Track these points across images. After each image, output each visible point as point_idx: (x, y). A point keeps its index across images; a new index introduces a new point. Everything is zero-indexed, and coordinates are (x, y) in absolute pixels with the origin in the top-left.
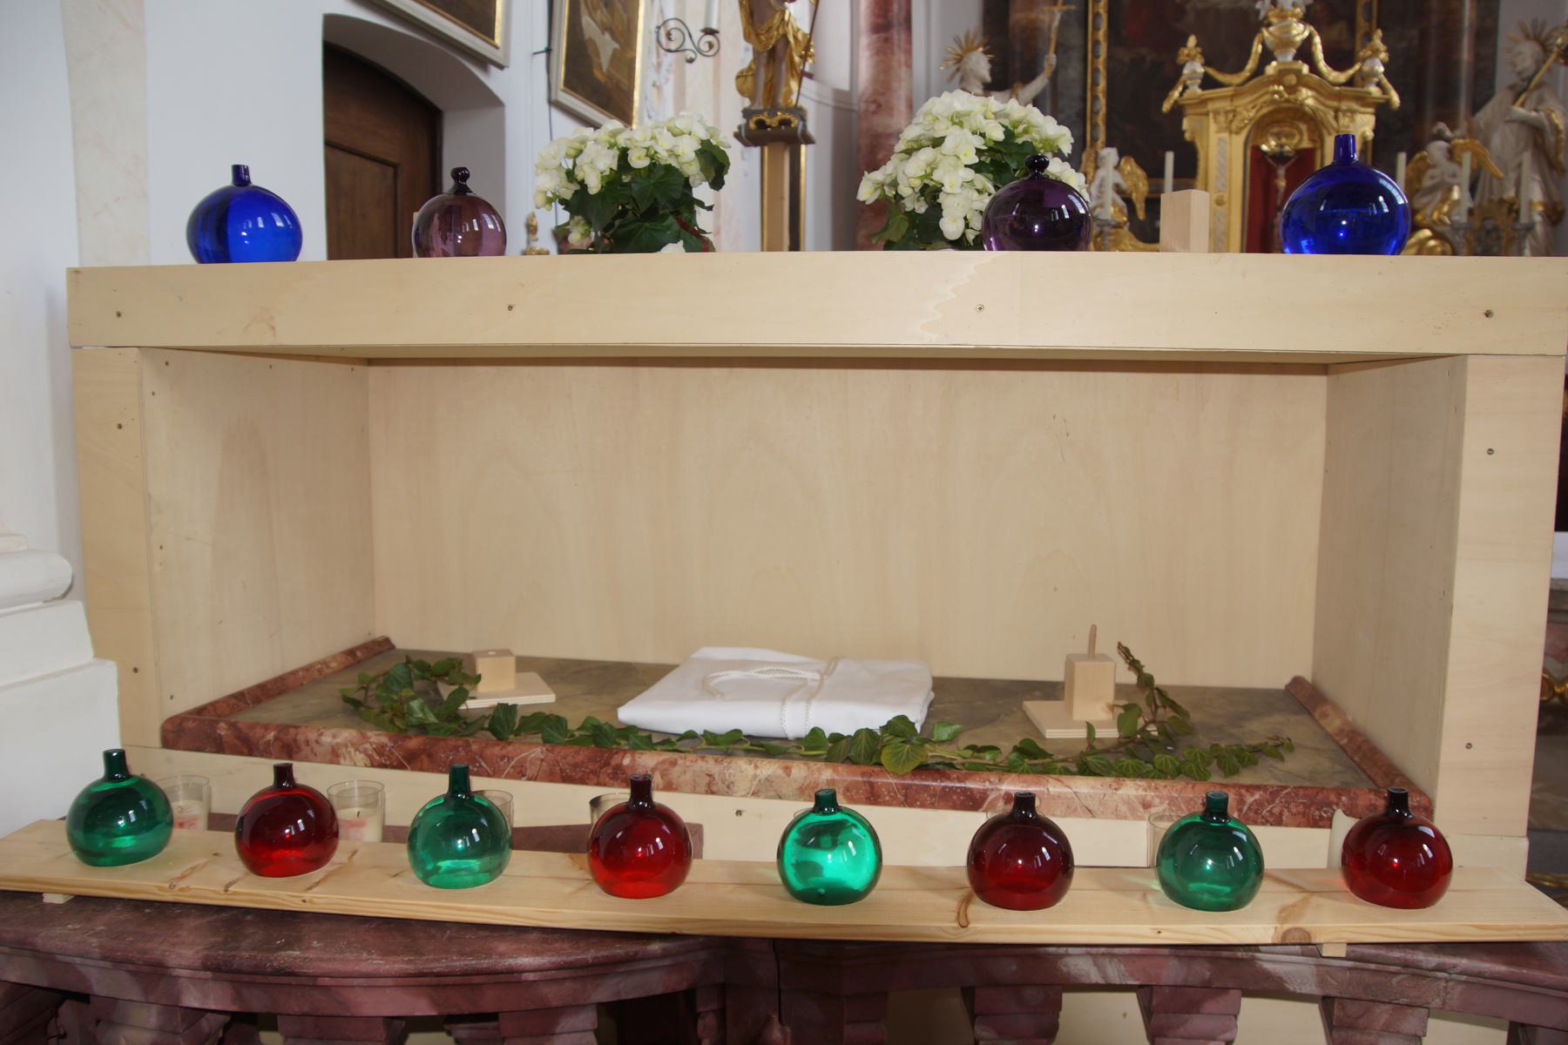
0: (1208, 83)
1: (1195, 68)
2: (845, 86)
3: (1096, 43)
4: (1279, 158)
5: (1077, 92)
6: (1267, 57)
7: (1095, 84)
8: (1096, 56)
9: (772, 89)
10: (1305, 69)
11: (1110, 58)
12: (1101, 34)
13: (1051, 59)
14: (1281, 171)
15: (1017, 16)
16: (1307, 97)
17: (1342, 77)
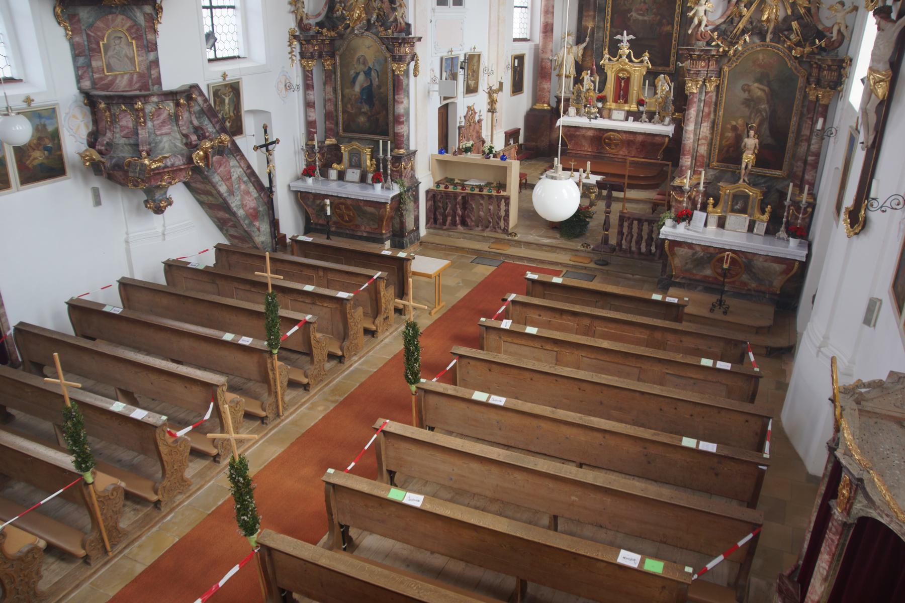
0: (610, 60)
1: (607, 56)
2: (538, 43)
3: (607, 27)
4: (623, 79)
5: (601, 39)
6: (621, 57)
7: (606, 38)
8: (607, 30)
9: (492, 105)
10: (627, 60)
11: (610, 31)
12: (608, 25)
13: (587, 39)
14: (623, 82)
15: (583, 23)
16: (627, 67)
17: (639, 60)
